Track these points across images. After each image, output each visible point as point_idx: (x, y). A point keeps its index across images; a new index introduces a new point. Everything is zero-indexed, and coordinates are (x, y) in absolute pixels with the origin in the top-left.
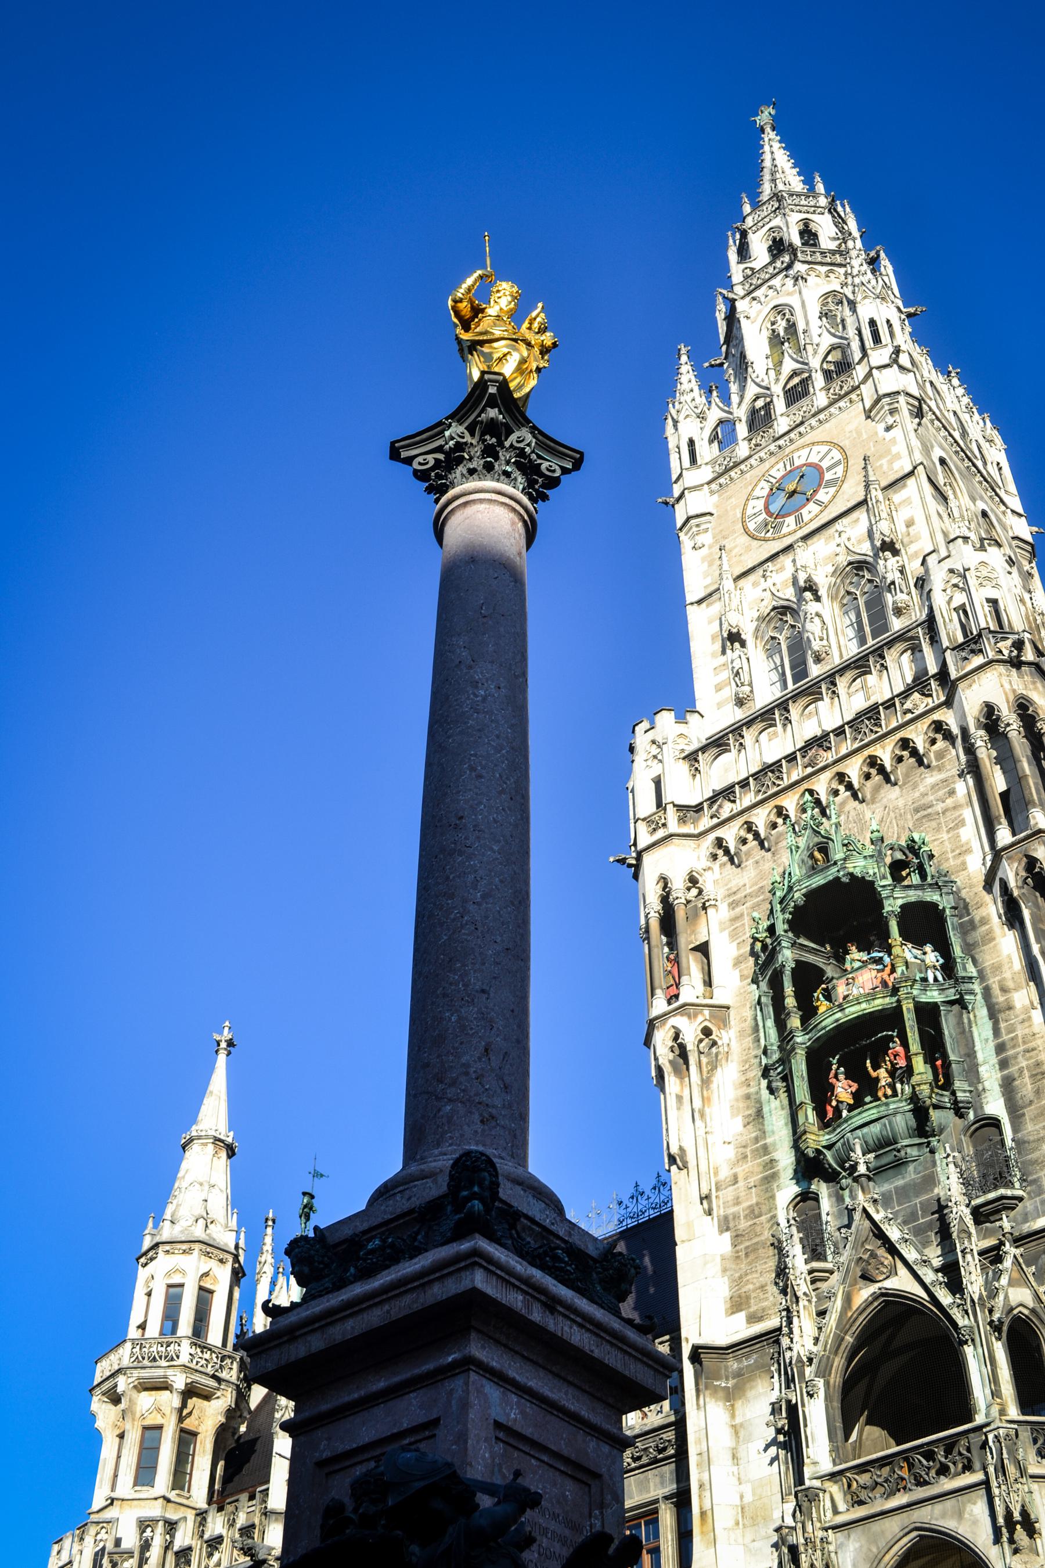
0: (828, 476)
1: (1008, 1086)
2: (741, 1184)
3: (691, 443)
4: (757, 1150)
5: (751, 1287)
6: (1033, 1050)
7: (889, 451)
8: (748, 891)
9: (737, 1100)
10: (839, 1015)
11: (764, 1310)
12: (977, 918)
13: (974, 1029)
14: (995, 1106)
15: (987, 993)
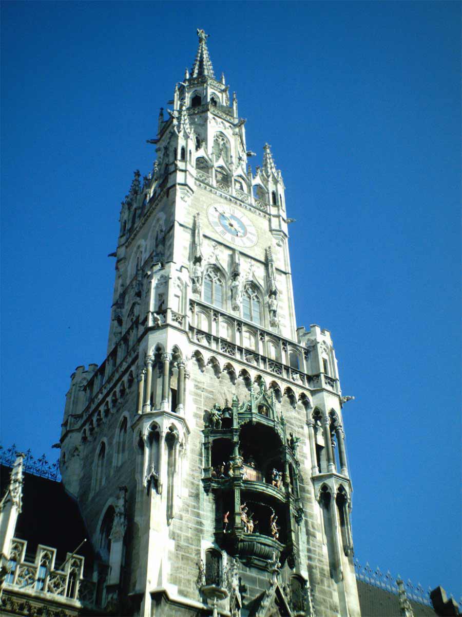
0: (248, 235)
1: (310, 568)
2: (184, 522)
3: (190, 151)
4: (195, 512)
5: (183, 576)
6: (322, 561)
7: (276, 254)
8: (205, 387)
9: (187, 480)
10: (264, 488)
11: (188, 592)
12: (306, 489)
13: (300, 534)
14: (305, 574)
15: (306, 522)
